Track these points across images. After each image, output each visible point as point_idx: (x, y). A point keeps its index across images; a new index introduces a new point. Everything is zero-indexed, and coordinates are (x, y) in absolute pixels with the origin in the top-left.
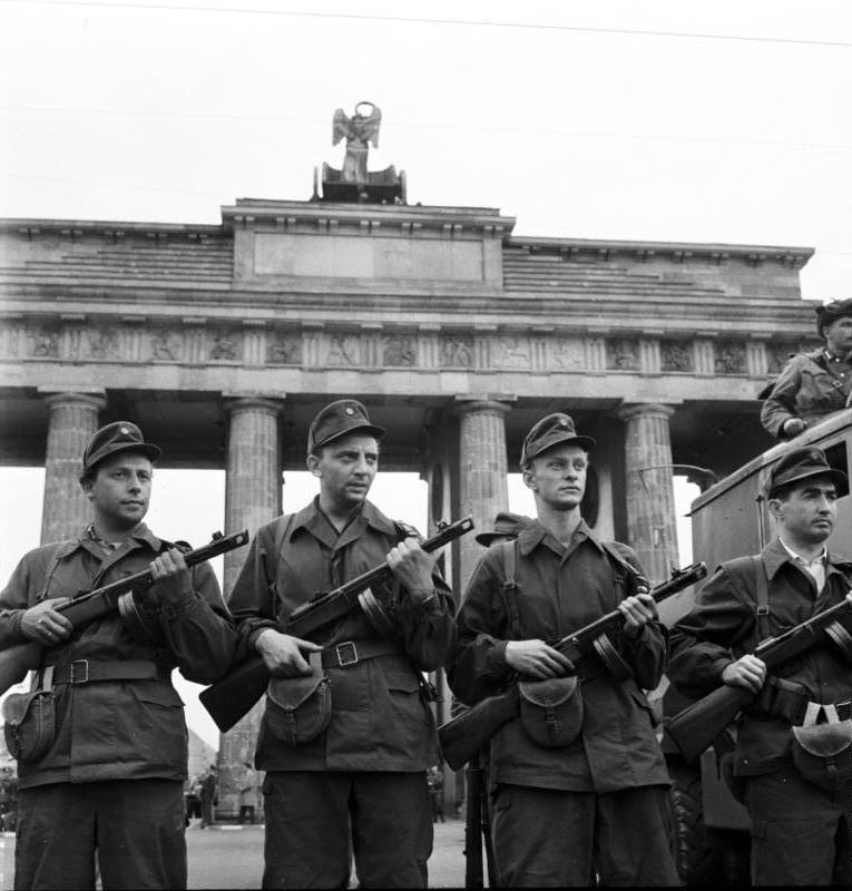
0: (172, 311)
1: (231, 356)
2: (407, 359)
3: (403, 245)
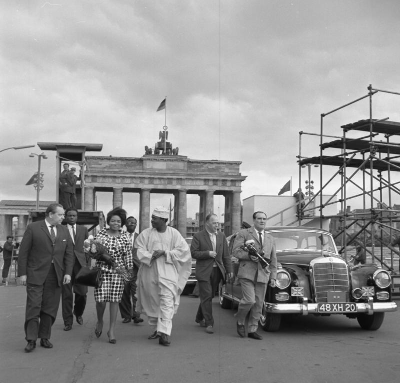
0: (134, 176)
1: (143, 182)
2: (171, 183)
3: (171, 163)
